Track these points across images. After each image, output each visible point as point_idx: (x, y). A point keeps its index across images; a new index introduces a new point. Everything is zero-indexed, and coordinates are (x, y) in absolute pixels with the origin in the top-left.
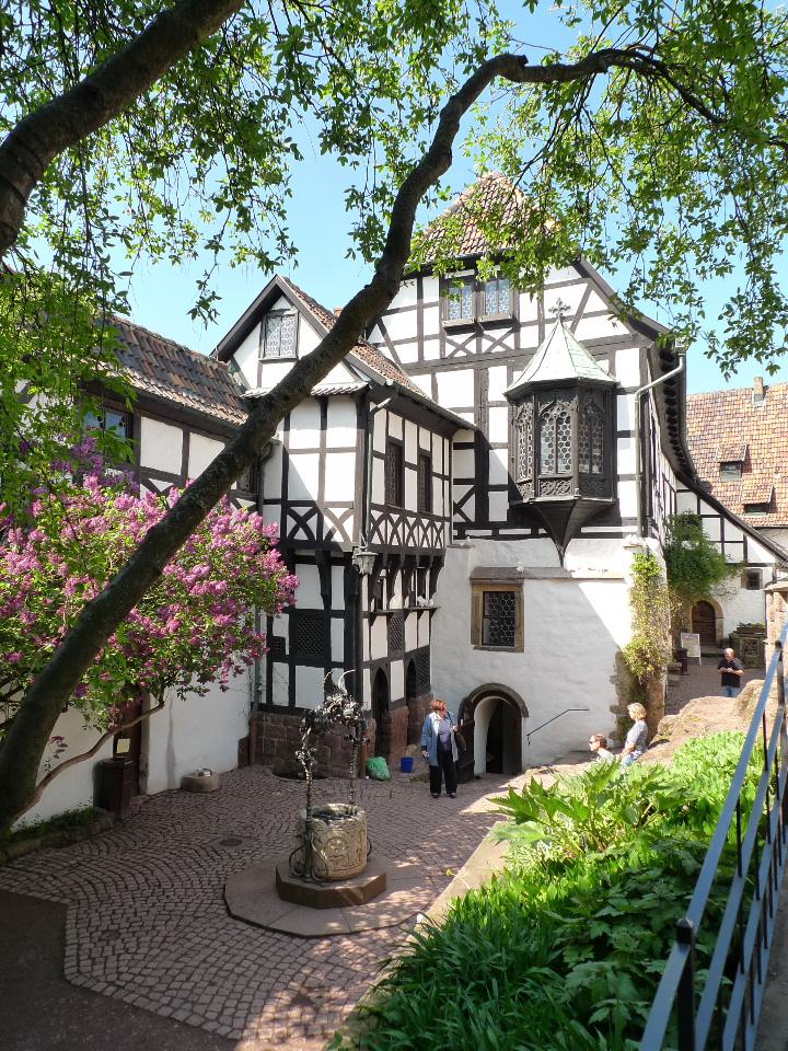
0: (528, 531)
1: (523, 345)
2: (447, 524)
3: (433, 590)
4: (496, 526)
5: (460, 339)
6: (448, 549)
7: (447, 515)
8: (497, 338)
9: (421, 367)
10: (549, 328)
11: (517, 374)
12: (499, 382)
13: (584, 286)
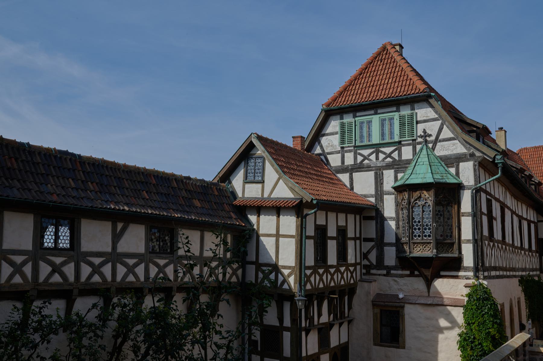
0: (408, 272)
1: (404, 157)
2: (358, 267)
3: (350, 308)
4: (389, 269)
6: (359, 283)
7: (358, 261)
10: (418, 147)
11: (400, 175)
12: (389, 179)
13: (439, 123)
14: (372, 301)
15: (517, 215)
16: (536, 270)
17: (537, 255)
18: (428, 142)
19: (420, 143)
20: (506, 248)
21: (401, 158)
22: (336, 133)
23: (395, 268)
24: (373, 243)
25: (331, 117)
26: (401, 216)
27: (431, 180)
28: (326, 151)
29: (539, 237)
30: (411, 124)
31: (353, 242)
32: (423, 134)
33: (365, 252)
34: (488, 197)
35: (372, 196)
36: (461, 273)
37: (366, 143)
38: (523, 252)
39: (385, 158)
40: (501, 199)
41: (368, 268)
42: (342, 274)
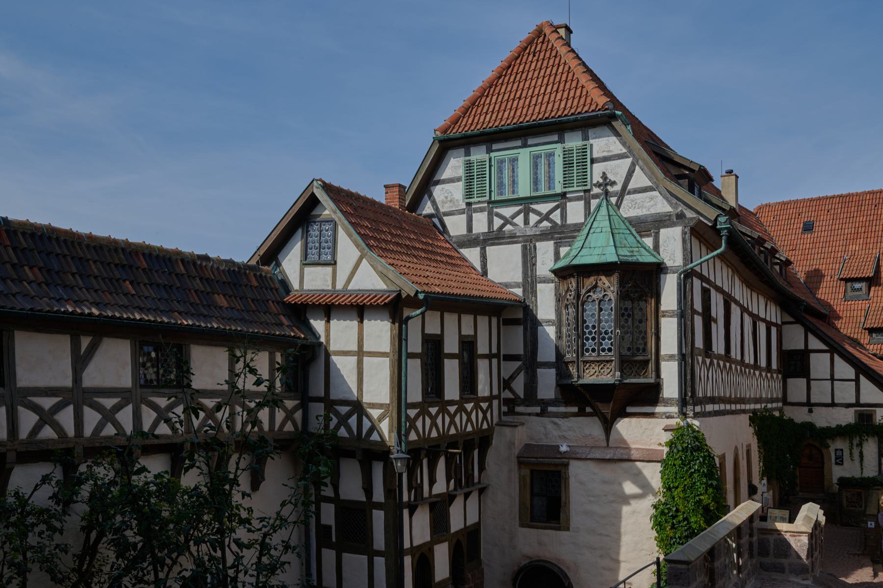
1: (570, 221)
2: (495, 403)
3: (482, 468)
4: (544, 404)
5: (507, 212)
7: (495, 392)
8: (544, 212)
9: (471, 241)
10: (594, 203)
11: (563, 251)
12: (546, 257)
14: (518, 457)
15: (751, 314)
16: (776, 400)
17: (780, 376)
18: (610, 194)
19: (596, 196)
20: (730, 367)
21: (566, 221)
22: (459, 179)
23: (554, 403)
24: (520, 363)
25: (450, 152)
26: (564, 318)
27: (613, 258)
28: (442, 210)
29: (784, 348)
30: (582, 164)
31: (487, 361)
32: (601, 181)
33: (506, 378)
34: (704, 285)
35: (517, 285)
36: (659, 409)
37: (508, 196)
38: (757, 373)
39: (540, 222)
40: (726, 289)
41: (511, 403)
42: (469, 415)
